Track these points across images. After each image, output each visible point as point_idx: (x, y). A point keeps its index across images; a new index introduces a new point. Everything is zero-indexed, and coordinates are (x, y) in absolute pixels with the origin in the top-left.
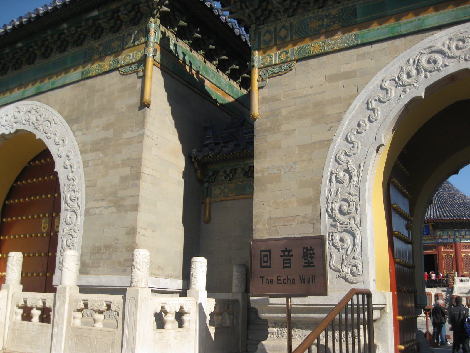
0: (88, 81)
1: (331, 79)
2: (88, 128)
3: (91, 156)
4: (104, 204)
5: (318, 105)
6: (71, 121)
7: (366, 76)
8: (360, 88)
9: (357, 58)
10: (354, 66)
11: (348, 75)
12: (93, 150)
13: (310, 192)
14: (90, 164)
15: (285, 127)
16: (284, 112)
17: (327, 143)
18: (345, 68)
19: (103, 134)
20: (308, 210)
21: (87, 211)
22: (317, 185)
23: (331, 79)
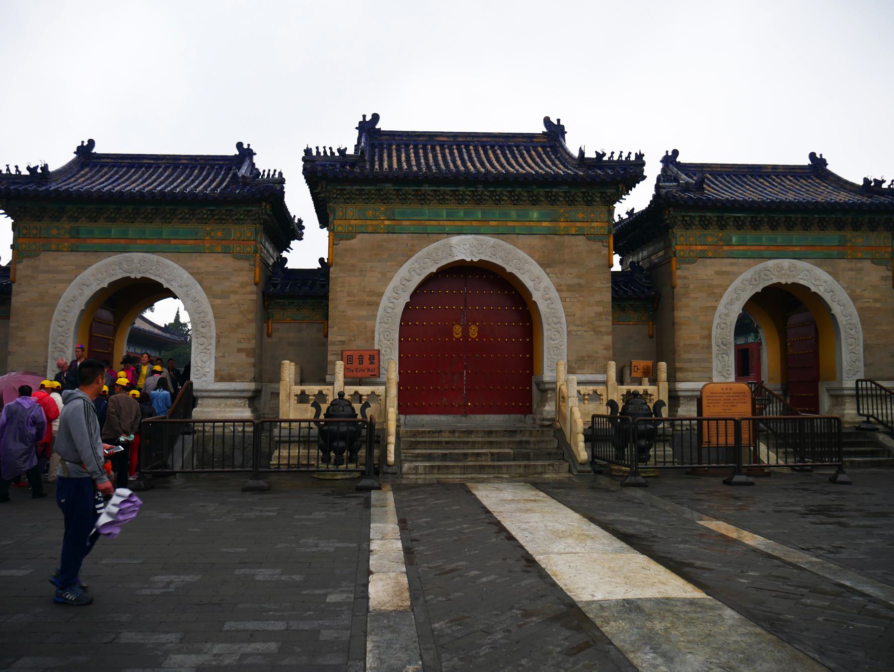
0: (556, 237)
1: (718, 273)
2: (561, 274)
3: (565, 294)
4: (584, 329)
5: (710, 286)
6: (544, 265)
7: (737, 275)
8: (731, 281)
9: (731, 264)
10: (729, 269)
11: (727, 273)
12: (568, 291)
13: (705, 333)
14: (568, 300)
15: (692, 295)
16: (691, 286)
17: (714, 308)
18: (724, 269)
19: (576, 281)
20: (705, 342)
21: (569, 333)
22: (710, 330)
23: (718, 273)
